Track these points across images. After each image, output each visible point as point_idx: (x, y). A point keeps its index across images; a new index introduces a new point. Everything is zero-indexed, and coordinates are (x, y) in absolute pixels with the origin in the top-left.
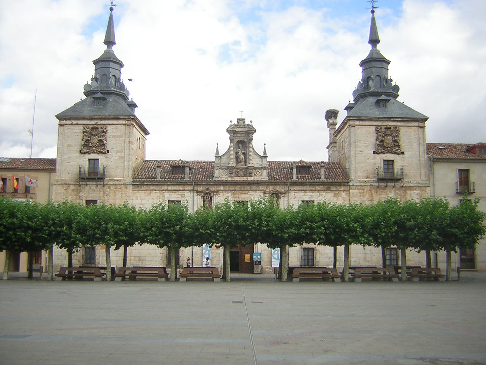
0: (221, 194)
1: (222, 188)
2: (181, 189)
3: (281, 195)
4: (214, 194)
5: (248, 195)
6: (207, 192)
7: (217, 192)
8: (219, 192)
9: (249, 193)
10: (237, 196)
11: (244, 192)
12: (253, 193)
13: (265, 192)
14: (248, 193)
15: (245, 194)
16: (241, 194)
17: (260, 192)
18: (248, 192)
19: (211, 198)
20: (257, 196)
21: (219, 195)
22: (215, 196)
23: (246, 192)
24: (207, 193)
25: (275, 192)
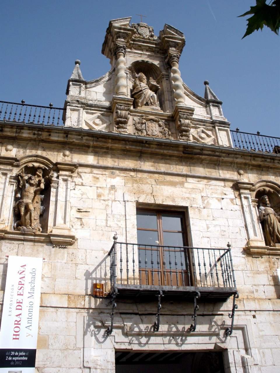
0: (87, 176)
1: (90, 159)
4: (61, 173)
5: (184, 190)
6: (36, 165)
8: (80, 169)
9: (186, 185)
10: (147, 188)
13: (237, 187)
14: (182, 184)
18: (184, 179)
20: (216, 196)
21: (78, 180)
22: (65, 180)
24: (32, 171)
25: (267, 189)
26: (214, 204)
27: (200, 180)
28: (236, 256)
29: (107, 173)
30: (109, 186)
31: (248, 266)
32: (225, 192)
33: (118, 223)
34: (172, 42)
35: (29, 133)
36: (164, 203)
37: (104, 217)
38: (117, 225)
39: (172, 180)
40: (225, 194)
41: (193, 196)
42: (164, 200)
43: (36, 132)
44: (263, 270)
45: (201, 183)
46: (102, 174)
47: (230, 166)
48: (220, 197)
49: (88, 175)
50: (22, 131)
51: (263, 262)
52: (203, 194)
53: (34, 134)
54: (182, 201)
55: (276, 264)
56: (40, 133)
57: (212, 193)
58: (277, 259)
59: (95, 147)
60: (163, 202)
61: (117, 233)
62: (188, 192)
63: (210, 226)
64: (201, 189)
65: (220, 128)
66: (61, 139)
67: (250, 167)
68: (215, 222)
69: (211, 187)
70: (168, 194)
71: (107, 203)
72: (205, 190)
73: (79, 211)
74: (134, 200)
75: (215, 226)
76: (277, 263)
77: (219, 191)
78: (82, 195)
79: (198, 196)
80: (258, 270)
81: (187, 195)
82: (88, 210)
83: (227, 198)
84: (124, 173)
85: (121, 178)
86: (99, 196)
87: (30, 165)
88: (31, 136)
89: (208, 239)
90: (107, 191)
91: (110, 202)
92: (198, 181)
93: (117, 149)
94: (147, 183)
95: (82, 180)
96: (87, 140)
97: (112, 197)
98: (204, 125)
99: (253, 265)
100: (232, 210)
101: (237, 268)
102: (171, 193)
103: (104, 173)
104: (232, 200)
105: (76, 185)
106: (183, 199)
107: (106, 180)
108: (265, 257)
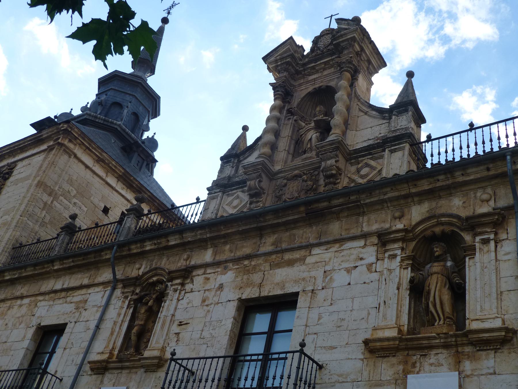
0: (198, 280)
2: (86, 282)
3: (475, 235)
6: (155, 279)
7: (186, 274)
9: (310, 260)
10: (257, 277)
11: (287, 256)
12: (327, 256)
13: (384, 239)
14: (302, 260)
15: (291, 263)
16: (279, 265)
17: (362, 243)
18: (303, 253)
19: (160, 299)
23: (297, 255)
26: (340, 278)
27: (329, 246)
28: (349, 359)
29: (219, 270)
30: (217, 286)
31: (365, 374)
32: (361, 256)
33: (213, 332)
34: (343, 41)
35: (151, 245)
36: (269, 295)
37: (200, 327)
38: (211, 334)
39: (291, 257)
40: (361, 259)
41: (313, 274)
42: (271, 290)
43: (156, 242)
44: (389, 378)
45: (330, 250)
46: (214, 273)
47: (382, 209)
48: (352, 265)
49: (200, 277)
50: (145, 244)
51: (394, 364)
52: (328, 268)
53: (155, 244)
54: (294, 285)
55: (418, 365)
56: (159, 241)
57: (342, 262)
58: (421, 355)
59: (212, 239)
60: (269, 292)
61: (209, 345)
62: (308, 269)
63: (323, 315)
64: (327, 260)
65: (393, 148)
66: (178, 242)
67: (416, 199)
68: (331, 309)
69: (342, 254)
70: (279, 280)
71: (208, 308)
72: (332, 261)
73: (180, 324)
74: (238, 297)
75: (331, 313)
76: (421, 363)
77: (353, 257)
78: (188, 303)
79: (319, 274)
80: (381, 380)
81: (306, 275)
82: (188, 322)
83: (362, 265)
84: (237, 265)
85: (233, 272)
86: (204, 301)
87: (151, 281)
88: (153, 247)
89: (316, 336)
90: (213, 293)
91: (212, 306)
92: (326, 250)
93: (234, 233)
94: (260, 270)
95: (193, 285)
96: (201, 234)
97: (216, 299)
98: (370, 154)
99: (374, 370)
100: (365, 283)
101: (346, 378)
102: (284, 278)
103: (217, 270)
104: (369, 267)
105: (185, 293)
106: (296, 281)
107: (216, 279)
108: (400, 356)
